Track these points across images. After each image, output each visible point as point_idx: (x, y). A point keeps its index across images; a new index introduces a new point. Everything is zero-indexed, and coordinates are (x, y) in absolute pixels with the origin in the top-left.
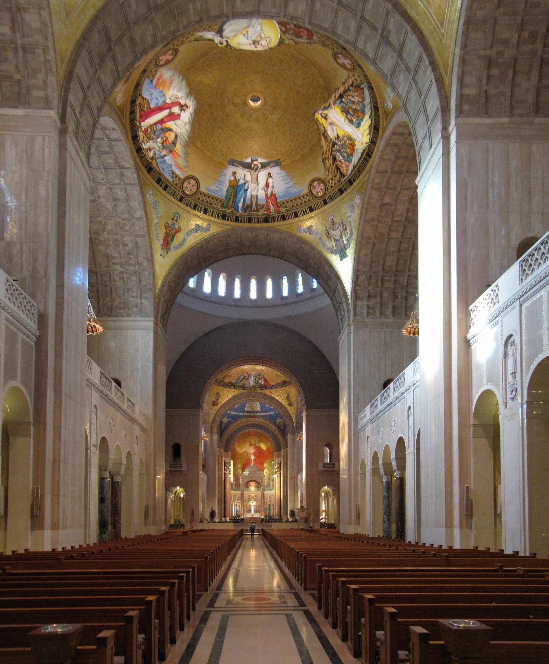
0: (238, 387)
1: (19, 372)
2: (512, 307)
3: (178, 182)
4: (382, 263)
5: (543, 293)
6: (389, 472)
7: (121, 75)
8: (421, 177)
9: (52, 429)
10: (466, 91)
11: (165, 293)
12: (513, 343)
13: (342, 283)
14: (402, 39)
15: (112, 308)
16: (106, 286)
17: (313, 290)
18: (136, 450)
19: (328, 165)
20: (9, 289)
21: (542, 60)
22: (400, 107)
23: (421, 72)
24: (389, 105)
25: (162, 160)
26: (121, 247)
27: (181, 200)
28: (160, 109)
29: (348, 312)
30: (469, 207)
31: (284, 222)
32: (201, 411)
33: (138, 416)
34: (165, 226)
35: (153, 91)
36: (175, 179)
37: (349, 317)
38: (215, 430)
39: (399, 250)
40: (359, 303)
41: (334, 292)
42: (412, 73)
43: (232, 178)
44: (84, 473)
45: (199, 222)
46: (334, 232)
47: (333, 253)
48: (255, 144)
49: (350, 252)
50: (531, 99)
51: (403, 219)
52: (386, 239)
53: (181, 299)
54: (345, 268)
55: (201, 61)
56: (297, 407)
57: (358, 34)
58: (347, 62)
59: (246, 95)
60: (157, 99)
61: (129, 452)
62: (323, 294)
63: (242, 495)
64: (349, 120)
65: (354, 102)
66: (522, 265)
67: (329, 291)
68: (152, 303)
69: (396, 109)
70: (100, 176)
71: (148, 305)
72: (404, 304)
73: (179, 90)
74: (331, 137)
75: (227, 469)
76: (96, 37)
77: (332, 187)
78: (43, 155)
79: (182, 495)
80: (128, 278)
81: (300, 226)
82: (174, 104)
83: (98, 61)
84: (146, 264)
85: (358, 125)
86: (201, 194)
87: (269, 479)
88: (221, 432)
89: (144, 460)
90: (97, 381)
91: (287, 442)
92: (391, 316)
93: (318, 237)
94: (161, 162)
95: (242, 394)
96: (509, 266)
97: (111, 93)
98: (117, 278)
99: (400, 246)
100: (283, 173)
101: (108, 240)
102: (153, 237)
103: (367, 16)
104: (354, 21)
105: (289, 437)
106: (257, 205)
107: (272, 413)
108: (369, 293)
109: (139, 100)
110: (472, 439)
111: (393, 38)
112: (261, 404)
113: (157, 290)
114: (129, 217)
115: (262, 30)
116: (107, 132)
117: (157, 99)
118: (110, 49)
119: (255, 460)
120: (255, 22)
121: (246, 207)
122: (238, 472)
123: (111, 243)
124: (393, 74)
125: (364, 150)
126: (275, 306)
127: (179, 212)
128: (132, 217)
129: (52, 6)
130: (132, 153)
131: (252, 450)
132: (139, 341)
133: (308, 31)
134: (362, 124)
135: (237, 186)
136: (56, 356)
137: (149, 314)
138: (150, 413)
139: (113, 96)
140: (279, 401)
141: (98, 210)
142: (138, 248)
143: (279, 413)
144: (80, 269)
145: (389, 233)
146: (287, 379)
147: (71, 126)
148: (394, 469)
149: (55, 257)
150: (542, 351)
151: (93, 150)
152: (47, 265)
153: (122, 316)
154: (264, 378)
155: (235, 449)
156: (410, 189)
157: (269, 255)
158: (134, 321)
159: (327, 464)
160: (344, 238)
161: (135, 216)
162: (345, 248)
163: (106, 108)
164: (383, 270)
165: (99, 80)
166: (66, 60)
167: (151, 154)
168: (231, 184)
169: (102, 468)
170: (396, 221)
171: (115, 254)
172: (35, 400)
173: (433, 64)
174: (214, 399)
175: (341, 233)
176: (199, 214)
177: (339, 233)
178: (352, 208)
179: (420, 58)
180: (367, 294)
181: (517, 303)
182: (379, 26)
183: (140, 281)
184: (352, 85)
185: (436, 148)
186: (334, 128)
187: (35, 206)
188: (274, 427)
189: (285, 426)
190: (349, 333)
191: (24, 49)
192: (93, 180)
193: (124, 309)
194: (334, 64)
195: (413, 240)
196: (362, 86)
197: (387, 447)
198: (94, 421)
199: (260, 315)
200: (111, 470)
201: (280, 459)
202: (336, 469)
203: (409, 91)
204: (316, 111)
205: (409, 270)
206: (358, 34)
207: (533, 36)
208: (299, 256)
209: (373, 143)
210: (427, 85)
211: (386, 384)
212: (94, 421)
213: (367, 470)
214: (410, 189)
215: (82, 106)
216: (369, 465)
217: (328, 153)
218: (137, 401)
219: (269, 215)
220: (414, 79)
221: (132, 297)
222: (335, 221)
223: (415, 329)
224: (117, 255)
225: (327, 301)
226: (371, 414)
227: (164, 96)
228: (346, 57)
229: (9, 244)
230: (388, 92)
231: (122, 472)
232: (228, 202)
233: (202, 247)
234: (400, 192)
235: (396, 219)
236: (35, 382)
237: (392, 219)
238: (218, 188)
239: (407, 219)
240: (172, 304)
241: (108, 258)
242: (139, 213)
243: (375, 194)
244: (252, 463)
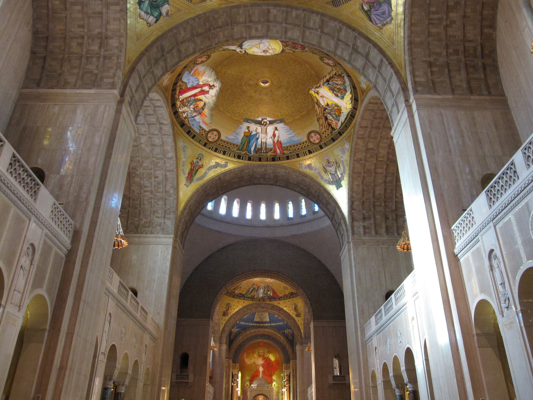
0: (248, 298)
1: (46, 281)
2: (487, 227)
3: (204, 133)
4: (372, 192)
5: (510, 216)
6: (401, 385)
7: (169, 69)
8: (395, 130)
9: (65, 335)
10: (418, 79)
11: (185, 215)
12: (496, 257)
13: (339, 207)
14: (367, 50)
15: (138, 227)
16: (136, 208)
17: (315, 213)
18: (143, 359)
19: (321, 122)
20: (54, 211)
21: (466, 64)
22: (371, 88)
23: (383, 68)
24: (364, 86)
26: (153, 178)
27: (205, 145)
28: (194, 88)
29: (347, 231)
30: (435, 152)
31: (288, 161)
32: (211, 321)
33: (150, 326)
34: (191, 163)
35: (190, 77)
36: (201, 131)
37: (348, 236)
38: (224, 340)
39: (385, 182)
40: (356, 224)
41: (334, 215)
42: (377, 69)
43: (247, 131)
44: (88, 382)
45: (218, 161)
46: (330, 169)
47: (330, 184)
49: (345, 183)
50: (465, 85)
51: (386, 159)
52: (374, 174)
53: (199, 220)
54: (341, 196)
55: (226, 61)
56: (304, 318)
57: (336, 47)
58: (330, 62)
59: (258, 80)
60: (193, 82)
61: (136, 361)
62: (324, 216)
64: (335, 94)
65: (337, 84)
66: (488, 195)
67: (328, 213)
68: (174, 223)
69: (368, 89)
70: (143, 129)
71: (170, 224)
72: (395, 225)
73: (210, 77)
74: (323, 104)
75: (235, 382)
76: (155, 50)
77: (325, 137)
78: (103, 117)
80: (155, 202)
81: (301, 164)
82: (204, 85)
83: (154, 62)
84: (172, 191)
85: (342, 98)
86: (221, 141)
87: (278, 393)
88: (230, 343)
89: (150, 371)
90: (115, 290)
91: (296, 353)
92: (385, 234)
93: (317, 172)
94: (192, 120)
95: (251, 305)
96: (478, 195)
97: (159, 79)
98: (146, 202)
99: (386, 179)
100: (286, 127)
101: (143, 173)
102: (180, 172)
103: (342, 38)
104: (333, 41)
105: (298, 348)
106: (266, 148)
107: (281, 323)
108: (363, 214)
109: (180, 83)
110: (477, 349)
111: (360, 50)
112: (269, 314)
113: (179, 212)
114: (163, 157)
115: (269, 45)
116: (154, 102)
117: (193, 82)
118: (163, 56)
119: (263, 372)
120: (264, 41)
121: (257, 150)
122: (246, 385)
123: (145, 176)
124: (364, 68)
125: (348, 113)
126: (282, 226)
127: (203, 154)
128: (165, 157)
129: (128, 35)
130: (170, 115)
131: (260, 361)
132: (159, 257)
133: (302, 46)
134: (345, 97)
135: (250, 136)
136: (82, 266)
137: (170, 231)
138: (161, 320)
139: (161, 81)
140: (287, 312)
141: (138, 152)
143: (287, 323)
144: (116, 195)
146: (294, 291)
147: (127, 99)
148: (405, 381)
149: (97, 187)
150: (522, 263)
151: (141, 113)
152: (89, 192)
153: (146, 233)
154: (273, 289)
155: (244, 361)
156: (387, 138)
157: (276, 185)
158: (156, 237)
159: (337, 376)
160: (338, 173)
161: (167, 156)
163: (155, 88)
164: (374, 196)
165: (153, 72)
166: (132, 62)
167: (185, 115)
168: (246, 134)
169: (107, 378)
170: (380, 161)
171: (147, 184)
172: (55, 307)
173: (391, 64)
174: (225, 310)
175: (336, 169)
176: (219, 155)
177: (334, 170)
178: (343, 152)
179: (382, 61)
180: (362, 216)
181: (491, 224)
182: (351, 44)
183: (165, 205)
184: (335, 74)
185: (403, 112)
186: (324, 99)
187: (89, 150)
188: (282, 338)
189: (293, 335)
190: (349, 250)
191: (105, 57)
192: (138, 132)
193: (149, 227)
194: (322, 63)
195: (395, 174)
196: (343, 75)
197: (396, 359)
198: (106, 329)
199: (268, 234)
200: (115, 379)
201: (289, 371)
202: (346, 382)
203: (377, 78)
204: (310, 89)
205: (396, 197)
206: (336, 47)
207: (456, 52)
208: (301, 186)
211: (388, 295)
212: (106, 329)
213: (378, 383)
214: (387, 138)
216: (380, 377)
217: (321, 115)
218: (151, 310)
219: (276, 156)
220: (379, 71)
221: (157, 217)
222: (330, 160)
223: (408, 246)
224: (149, 185)
225: (327, 222)
226: (377, 323)
227: (198, 80)
228: (329, 59)
229: (63, 177)
230: (362, 79)
231: (127, 382)
232: (243, 147)
233: (220, 179)
234: (380, 141)
235: (379, 159)
236: (59, 291)
237: (377, 159)
238: (235, 136)
239: (388, 159)
240: (191, 224)
241: (141, 186)
242: (171, 154)
243: (360, 142)
244: (261, 376)
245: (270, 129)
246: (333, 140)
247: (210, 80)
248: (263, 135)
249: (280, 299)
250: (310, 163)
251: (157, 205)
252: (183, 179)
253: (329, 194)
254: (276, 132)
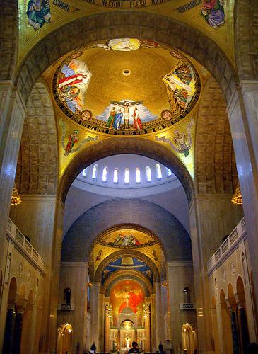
27: (80, 123)
39: (223, 150)
40: (200, 183)
48: (126, 93)
49: (191, 151)
53: (75, 184)
63: (119, 332)
79: (70, 331)
82: (79, 75)
84: (54, 161)
97: (44, 71)
100: (144, 107)
102: (60, 145)
105: (156, 284)
106: (128, 125)
119: (129, 304)
120: (125, 39)
121: (121, 127)
124: (204, 60)
139: (45, 73)
142: (50, 150)
145: (215, 141)
146: (153, 240)
147: (19, 87)
162: (188, 149)
167: (63, 100)
190: (195, 205)
209: (198, 92)
210: (224, 65)
215: (27, 78)
233: (92, 150)
238: (104, 115)
239: (225, 133)
242: (53, 131)
245: (132, 109)
246: (182, 117)
247: (83, 71)
248: (126, 114)
249: (141, 246)
250: (163, 135)
251: (43, 171)
252: (63, 151)
253: (179, 160)
254: (136, 111)
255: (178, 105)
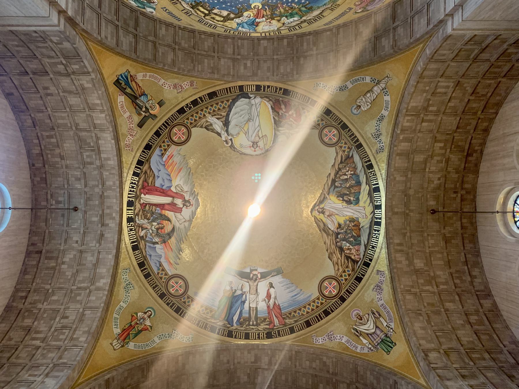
25: (152, 245)
77: (346, 280)
94: (150, 247)
248: (252, 296)
255: (348, 258)
